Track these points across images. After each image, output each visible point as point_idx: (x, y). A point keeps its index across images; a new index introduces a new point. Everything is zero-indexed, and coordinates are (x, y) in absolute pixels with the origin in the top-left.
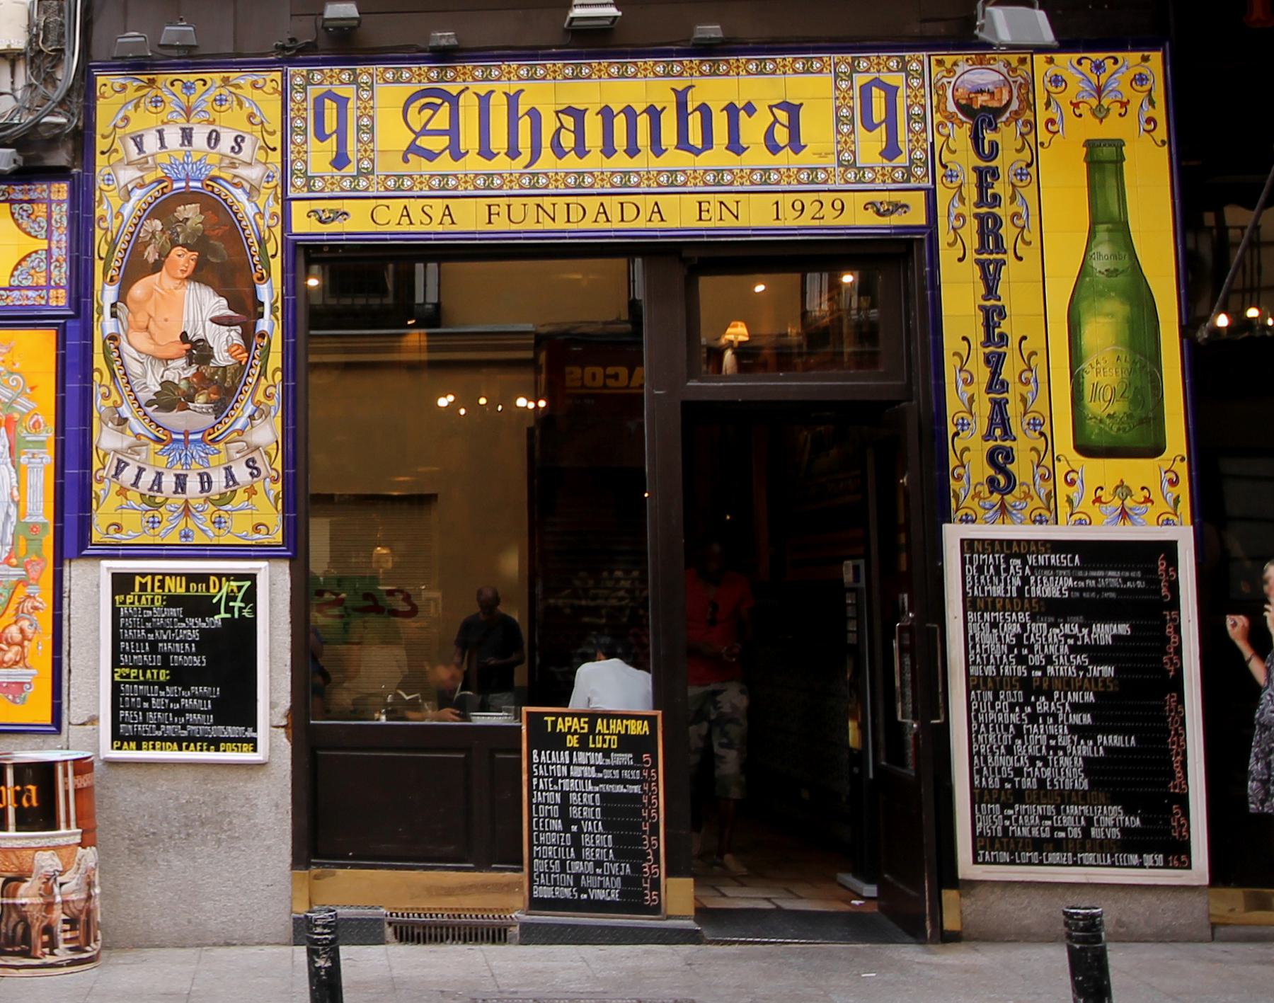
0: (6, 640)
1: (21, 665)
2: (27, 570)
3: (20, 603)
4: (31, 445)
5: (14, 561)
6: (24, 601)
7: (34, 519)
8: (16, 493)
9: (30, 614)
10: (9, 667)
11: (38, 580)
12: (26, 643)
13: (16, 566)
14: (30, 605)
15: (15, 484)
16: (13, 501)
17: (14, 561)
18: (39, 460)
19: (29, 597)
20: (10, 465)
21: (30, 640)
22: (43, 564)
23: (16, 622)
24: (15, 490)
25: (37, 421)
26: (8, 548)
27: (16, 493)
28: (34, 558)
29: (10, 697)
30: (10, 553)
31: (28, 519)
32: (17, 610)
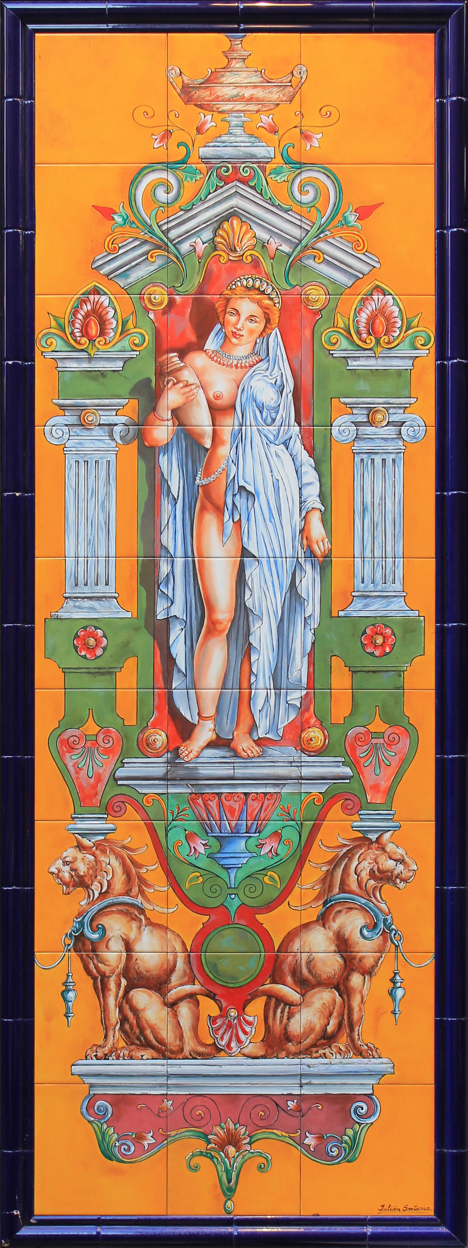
0: (295, 972)
1: (342, 1042)
2: (355, 764)
3: (335, 863)
4: (362, 385)
5: (315, 735)
6: (349, 855)
7: (376, 608)
8: (317, 529)
9: (368, 894)
10: (307, 1052)
11: (390, 791)
12: (356, 980)
13: (320, 752)
14: (366, 866)
15: (314, 501)
16: (311, 554)
17: (315, 735)
18: (391, 431)
19: (363, 841)
20: (297, 446)
21: (368, 972)
22: (404, 744)
23: (323, 919)
24: (315, 520)
25: (381, 311)
26: (295, 697)
27: (317, 529)
28: (378, 726)
29: (310, 1140)
30: (303, 709)
31: (357, 609)
32: (327, 880)
